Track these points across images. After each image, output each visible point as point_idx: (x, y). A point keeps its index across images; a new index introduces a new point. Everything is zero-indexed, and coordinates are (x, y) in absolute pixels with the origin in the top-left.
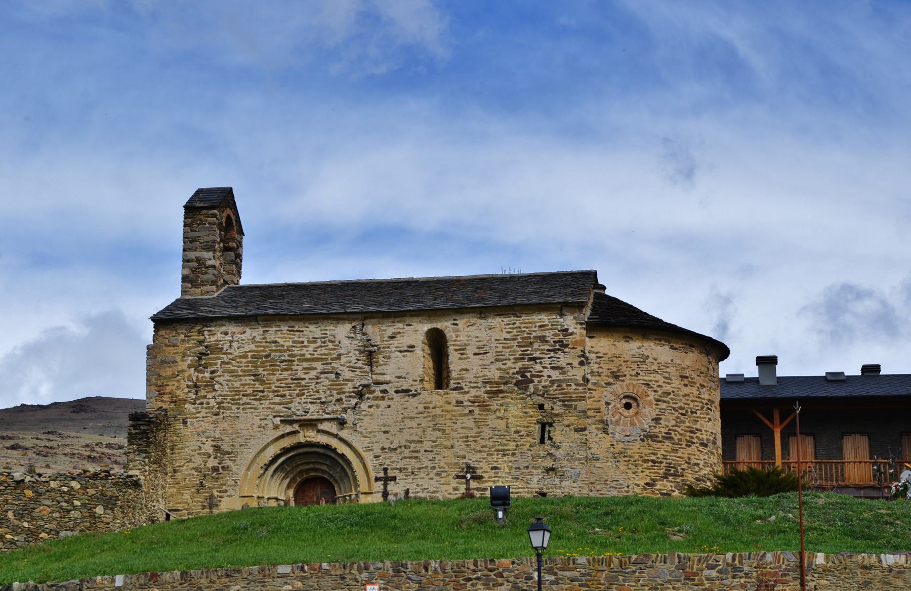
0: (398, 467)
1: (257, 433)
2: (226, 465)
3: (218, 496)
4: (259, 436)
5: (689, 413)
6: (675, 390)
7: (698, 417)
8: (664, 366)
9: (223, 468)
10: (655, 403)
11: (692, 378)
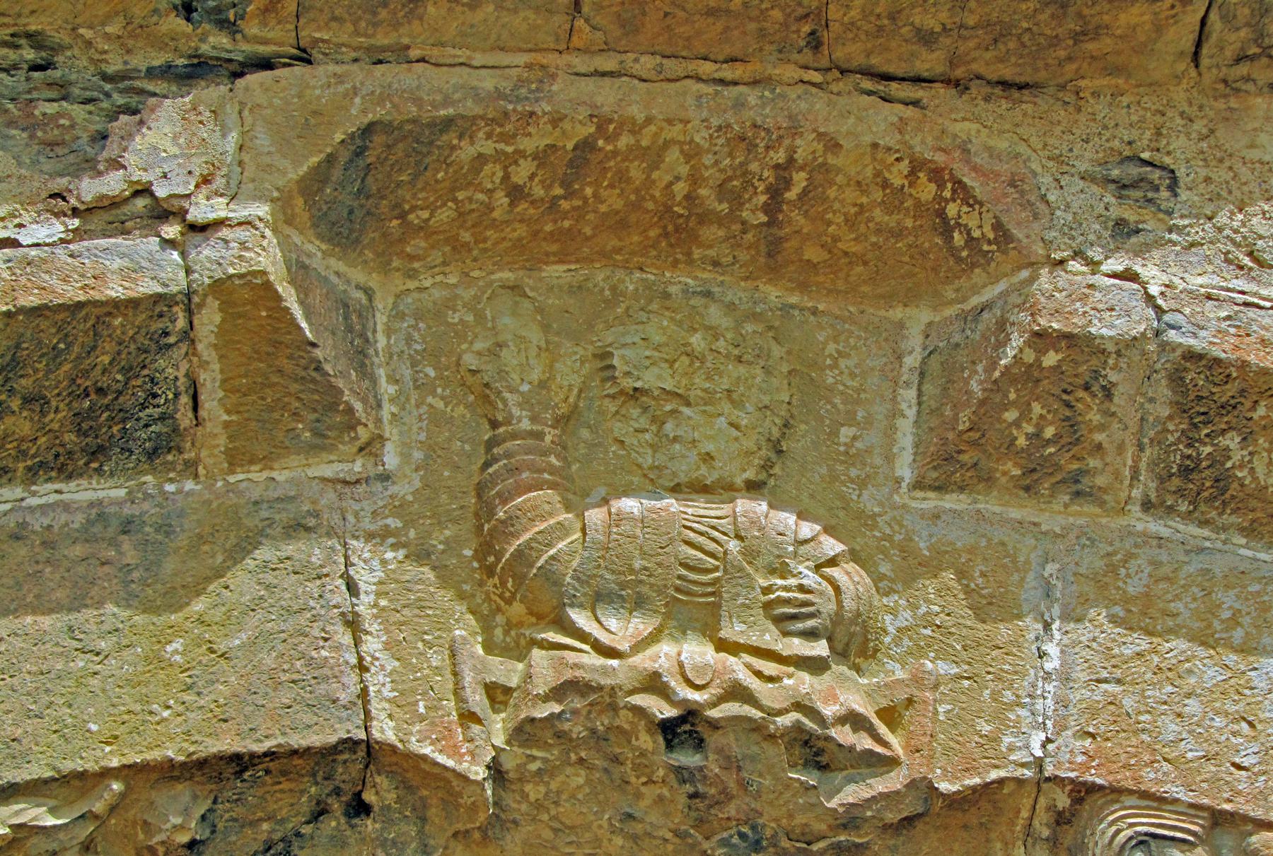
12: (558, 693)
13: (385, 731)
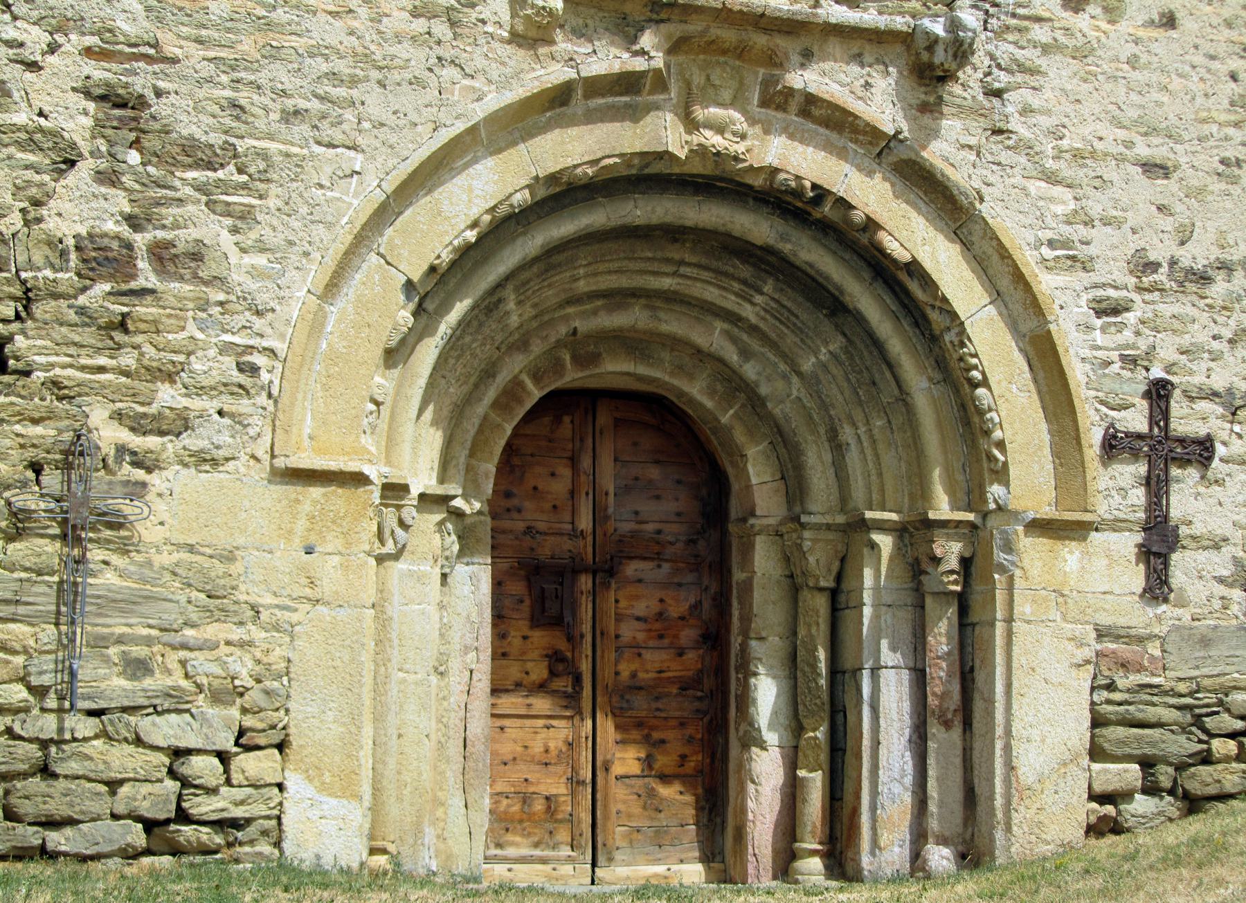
0: (1219, 382)
1: (404, 51)
2: (184, 238)
3: (121, 450)
4: (419, 71)
9: (162, 255)
12: (698, 145)
13: (670, 149)
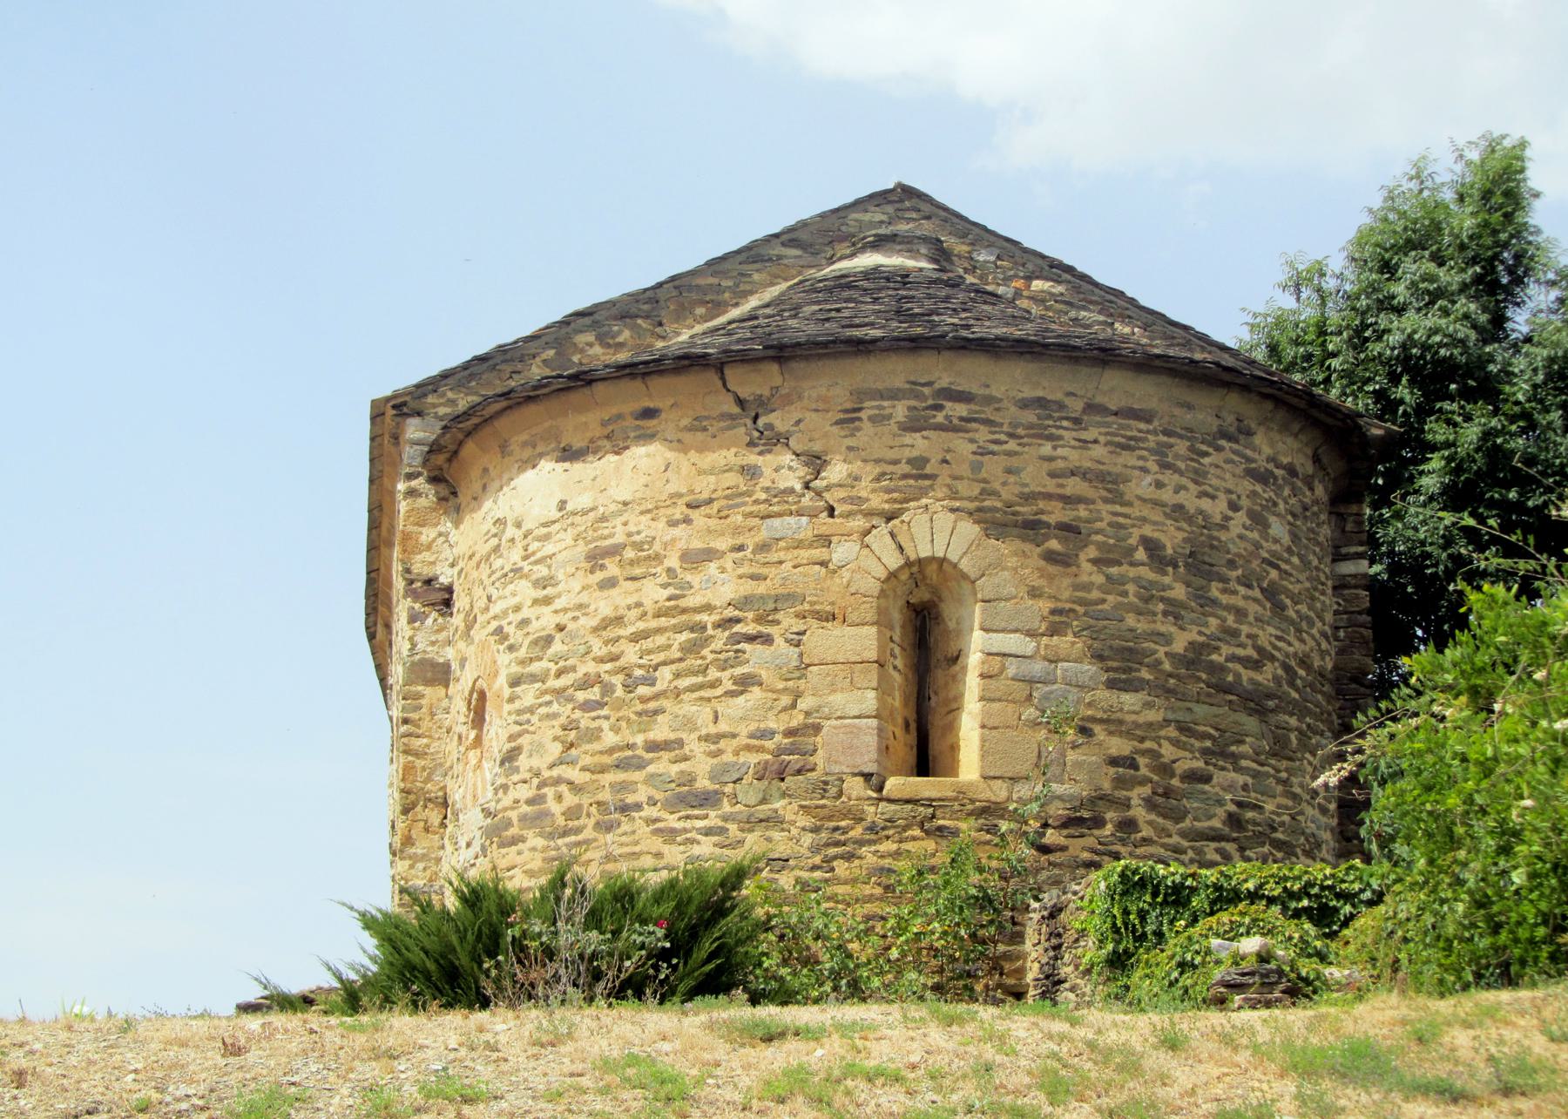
5: (619, 692)
6: (563, 619)
7: (656, 697)
8: (539, 539)
10: (507, 692)
11: (638, 546)
